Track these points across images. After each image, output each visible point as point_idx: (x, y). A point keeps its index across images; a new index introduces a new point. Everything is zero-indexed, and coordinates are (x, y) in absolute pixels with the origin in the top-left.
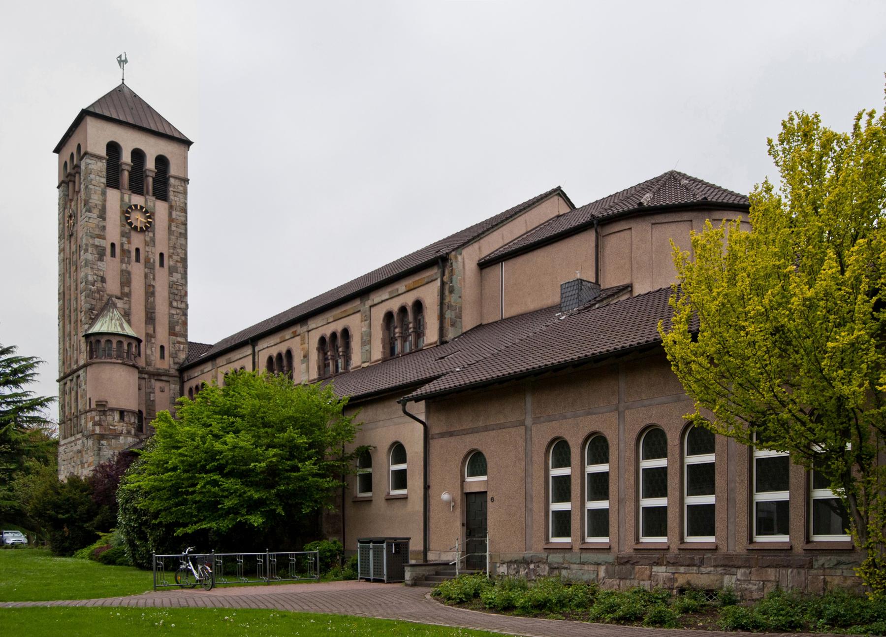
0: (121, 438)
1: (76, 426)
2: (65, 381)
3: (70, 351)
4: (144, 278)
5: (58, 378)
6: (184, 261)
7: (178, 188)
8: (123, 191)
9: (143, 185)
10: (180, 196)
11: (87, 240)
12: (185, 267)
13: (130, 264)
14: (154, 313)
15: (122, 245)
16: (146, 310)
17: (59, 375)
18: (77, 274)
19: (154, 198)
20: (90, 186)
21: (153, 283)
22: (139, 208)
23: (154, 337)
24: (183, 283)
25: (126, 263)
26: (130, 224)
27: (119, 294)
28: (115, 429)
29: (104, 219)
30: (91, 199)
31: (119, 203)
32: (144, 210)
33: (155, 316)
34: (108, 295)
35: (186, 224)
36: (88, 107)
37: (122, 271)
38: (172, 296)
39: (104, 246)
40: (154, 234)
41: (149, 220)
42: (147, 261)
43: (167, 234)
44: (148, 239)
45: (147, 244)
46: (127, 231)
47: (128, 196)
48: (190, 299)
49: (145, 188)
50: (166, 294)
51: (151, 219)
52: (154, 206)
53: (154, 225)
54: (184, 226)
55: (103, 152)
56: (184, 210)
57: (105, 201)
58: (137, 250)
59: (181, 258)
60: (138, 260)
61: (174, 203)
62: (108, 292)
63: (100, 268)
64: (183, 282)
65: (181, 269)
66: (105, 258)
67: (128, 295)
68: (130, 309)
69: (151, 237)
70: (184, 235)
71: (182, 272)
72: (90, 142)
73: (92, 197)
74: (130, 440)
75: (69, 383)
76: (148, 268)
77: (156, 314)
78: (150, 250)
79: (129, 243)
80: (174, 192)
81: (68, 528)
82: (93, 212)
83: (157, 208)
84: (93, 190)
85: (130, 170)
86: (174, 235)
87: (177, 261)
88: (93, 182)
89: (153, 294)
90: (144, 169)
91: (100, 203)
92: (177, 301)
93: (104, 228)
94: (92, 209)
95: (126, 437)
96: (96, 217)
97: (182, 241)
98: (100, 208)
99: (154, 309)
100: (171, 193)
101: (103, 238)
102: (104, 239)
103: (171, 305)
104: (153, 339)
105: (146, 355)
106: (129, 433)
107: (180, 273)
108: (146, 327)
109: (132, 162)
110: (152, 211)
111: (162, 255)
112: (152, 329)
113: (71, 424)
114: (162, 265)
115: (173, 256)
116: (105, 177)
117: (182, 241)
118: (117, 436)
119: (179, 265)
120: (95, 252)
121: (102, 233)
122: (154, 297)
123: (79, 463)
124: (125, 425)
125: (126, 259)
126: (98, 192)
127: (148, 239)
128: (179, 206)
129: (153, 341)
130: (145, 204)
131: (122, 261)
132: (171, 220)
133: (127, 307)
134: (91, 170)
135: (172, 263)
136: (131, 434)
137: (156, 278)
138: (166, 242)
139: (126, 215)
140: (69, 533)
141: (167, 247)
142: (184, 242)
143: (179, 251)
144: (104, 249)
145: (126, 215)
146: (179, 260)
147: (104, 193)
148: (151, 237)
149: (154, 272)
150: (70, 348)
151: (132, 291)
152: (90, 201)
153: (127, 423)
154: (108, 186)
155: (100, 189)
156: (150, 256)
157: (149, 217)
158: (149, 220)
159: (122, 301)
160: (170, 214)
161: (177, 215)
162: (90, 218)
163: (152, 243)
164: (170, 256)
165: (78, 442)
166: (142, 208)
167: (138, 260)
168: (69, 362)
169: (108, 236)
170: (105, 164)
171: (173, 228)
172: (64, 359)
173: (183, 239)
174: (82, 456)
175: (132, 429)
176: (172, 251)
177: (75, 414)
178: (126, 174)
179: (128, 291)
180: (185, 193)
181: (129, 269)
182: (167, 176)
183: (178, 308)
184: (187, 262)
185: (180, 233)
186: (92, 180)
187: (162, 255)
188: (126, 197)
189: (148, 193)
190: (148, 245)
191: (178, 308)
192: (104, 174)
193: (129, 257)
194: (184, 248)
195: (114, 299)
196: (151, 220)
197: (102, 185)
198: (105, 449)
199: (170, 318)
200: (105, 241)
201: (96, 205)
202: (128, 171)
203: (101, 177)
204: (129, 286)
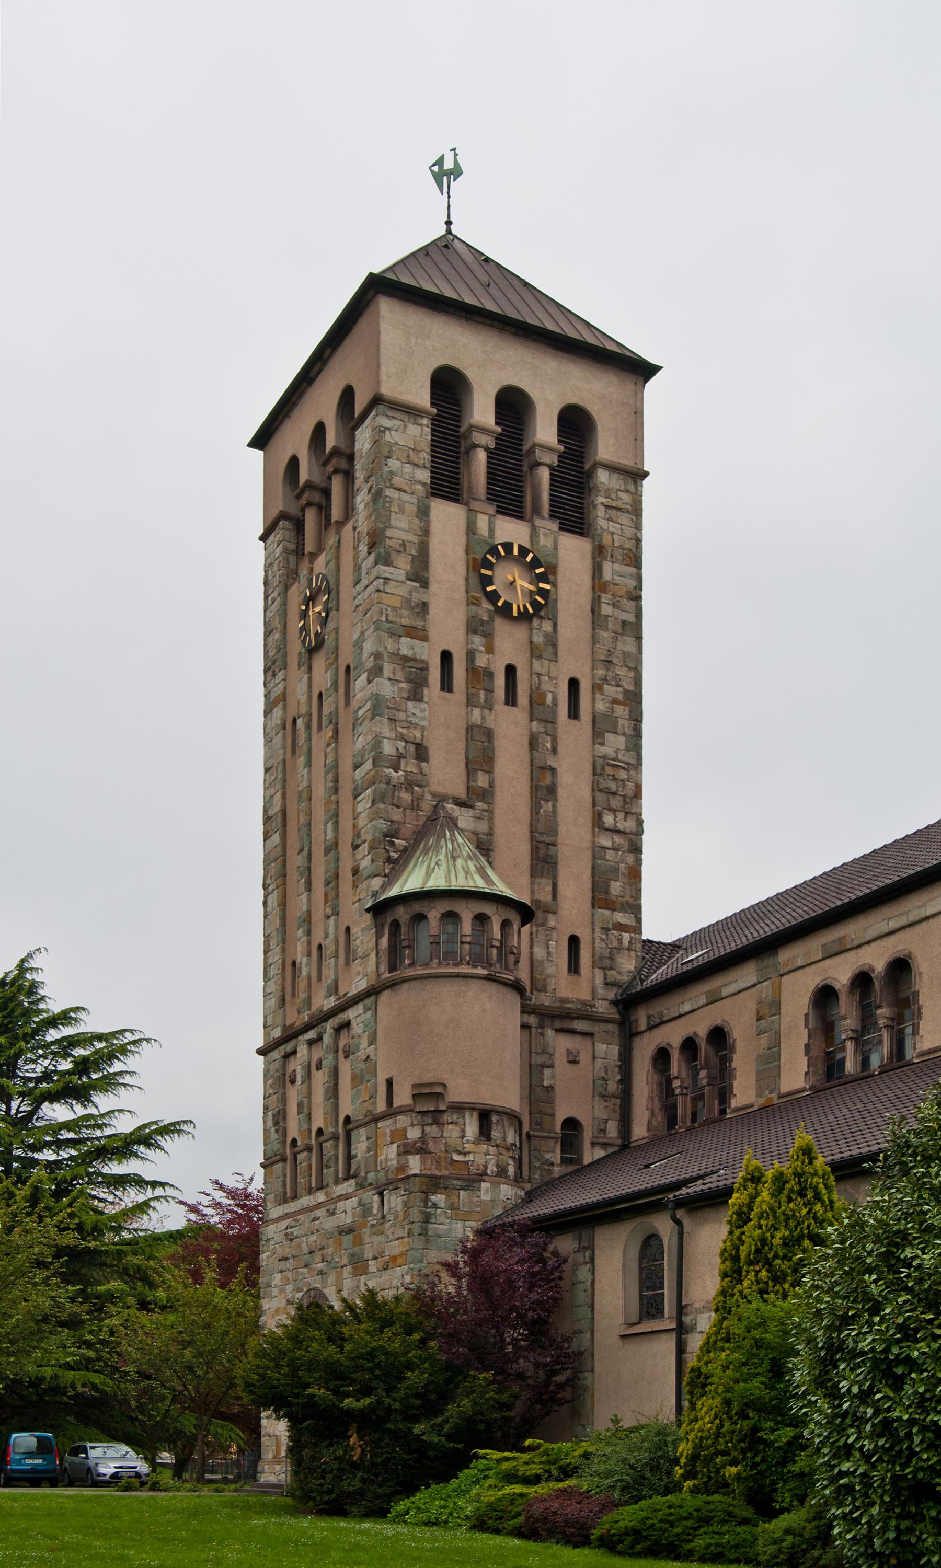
0: (485, 1186)
1: (332, 1163)
2: (289, 1047)
3: (308, 964)
4: (527, 747)
5: (260, 1043)
6: (634, 699)
7: (618, 498)
8: (475, 505)
9: (521, 490)
10: (624, 519)
11: (379, 641)
12: (637, 718)
13: (491, 709)
14: (554, 845)
15: (471, 655)
16: (532, 838)
17: (266, 1035)
18: (336, 750)
19: (554, 526)
20: (388, 492)
21: (551, 762)
22: (516, 552)
23: (554, 913)
24: (632, 762)
25: (483, 707)
26: (493, 597)
27: (462, 794)
28: (466, 1163)
29: (425, 584)
30: (391, 527)
31: (462, 540)
32: (528, 559)
33: (557, 852)
34: (434, 795)
35: (638, 599)
36: (391, 268)
37: (470, 729)
38: (600, 797)
39: (424, 657)
40: (555, 625)
41: (541, 585)
42: (537, 699)
43: (589, 626)
44: (538, 639)
45: (535, 652)
46: (485, 618)
47: (486, 518)
48: (649, 807)
49: (528, 499)
50: (585, 792)
51: (548, 583)
52: (556, 548)
53: (556, 600)
54: (634, 603)
55: (422, 397)
56: (635, 560)
57: (426, 532)
58: (510, 671)
59: (626, 692)
60: (511, 699)
61: (606, 540)
62: (435, 788)
63: (414, 720)
64: (629, 758)
65: (624, 724)
66: (426, 691)
67: (487, 795)
68: (490, 834)
69: (546, 635)
70: (634, 629)
71: (629, 731)
72: (388, 368)
73: (393, 522)
74: (507, 1192)
75: (303, 1050)
76: (540, 720)
77: (559, 846)
78: (544, 671)
79: (490, 650)
80: (607, 507)
81: (360, 1438)
82: (396, 563)
83: (562, 553)
84: (396, 502)
85: (492, 445)
86: (607, 630)
87: (615, 701)
88: (397, 481)
89: (552, 791)
90: (526, 448)
91: (415, 539)
92: (613, 811)
93: (424, 606)
94: (394, 555)
95: (496, 1185)
96: (403, 578)
97: (627, 644)
98: (414, 553)
99: (554, 832)
100: (601, 512)
101: (419, 634)
102: (425, 638)
103: (597, 822)
104: (550, 916)
105: (532, 961)
106: (502, 1172)
107: (624, 734)
108: (532, 884)
109: (497, 423)
110: (551, 560)
111: (574, 684)
112: (549, 888)
113: (310, 1159)
114: (574, 713)
115: (606, 687)
116: (428, 465)
117: (627, 644)
118: (472, 1180)
119: (621, 711)
120: (400, 676)
121: (419, 623)
122: (556, 800)
123: (345, 1261)
124: (492, 1150)
125: (482, 694)
126: (408, 507)
127: (538, 639)
128: (621, 547)
129: (552, 923)
130: (532, 544)
131: (470, 702)
132: (599, 585)
133: (483, 827)
134: (390, 445)
135: (601, 706)
136: (507, 1177)
137: (560, 749)
138: (586, 647)
139: (483, 571)
140: (363, 1450)
141: (589, 662)
142: (633, 649)
143: (621, 672)
144: (425, 668)
145: (483, 571)
146: (620, 697)
147: (423, 513)
148: (546, 635)
149: (555, 729)
150: (309, 955)
151: (497, 783)
152: (388, 533)
153: (497, 1146)
154: (433, 494)
155: (415, 501)
156: (544, 687)
157: (543, 578)
158: (541, 585)
159: (471, 812)
160: (597, 570)
161: (614, 572)
162: (387, 579)
163: (550, 649)
164: (597, 688)
165: (340, 1204)
166: (523, 551)
167: (511, 699)
168: (303, 995)
169: (433, 633)
170: (428, 430)
171: (606, 609)
172: (283, 989)
173: (630, 640)
174: (358, 1242)
175: (511, 1162)
176: (601, 672)
177: (329, 1130)
178: (481, 457)
179: (486, 785)
180: (636, 510)
181: (489, 723)
182: (587, 466)
183: (618, 832)
184: (641, 703)
185: (624, 623)
186: (392, 473)
187: (574, 684)
188: (482, 522)
189: (536, 511)
190: (540, 657)
191: (618, 832)
192: (425, 457)
193: (490, 691)
194: (635, 664)
195: (449, 806)
196: (547, 587)
197: (419, 487)
198: (442, 1219)
199: (594, 858)
200: (425, 644)
201: (404, 544)
202: (487, 449)
203: (417, 465)
204: (490, 772)
